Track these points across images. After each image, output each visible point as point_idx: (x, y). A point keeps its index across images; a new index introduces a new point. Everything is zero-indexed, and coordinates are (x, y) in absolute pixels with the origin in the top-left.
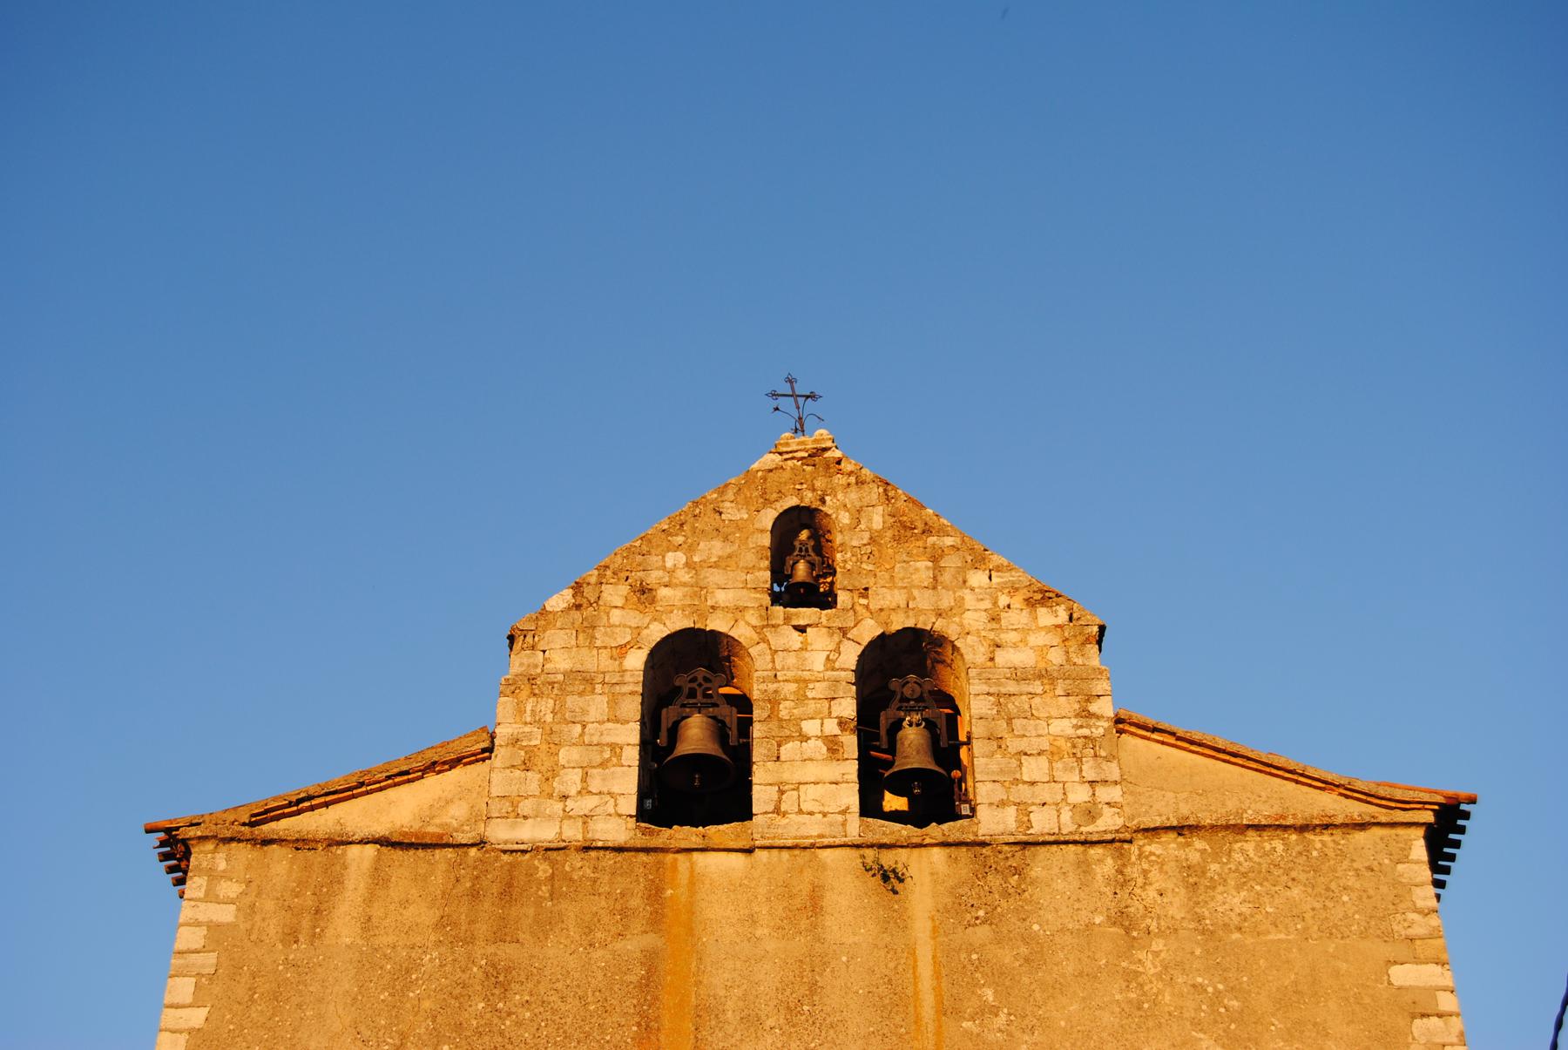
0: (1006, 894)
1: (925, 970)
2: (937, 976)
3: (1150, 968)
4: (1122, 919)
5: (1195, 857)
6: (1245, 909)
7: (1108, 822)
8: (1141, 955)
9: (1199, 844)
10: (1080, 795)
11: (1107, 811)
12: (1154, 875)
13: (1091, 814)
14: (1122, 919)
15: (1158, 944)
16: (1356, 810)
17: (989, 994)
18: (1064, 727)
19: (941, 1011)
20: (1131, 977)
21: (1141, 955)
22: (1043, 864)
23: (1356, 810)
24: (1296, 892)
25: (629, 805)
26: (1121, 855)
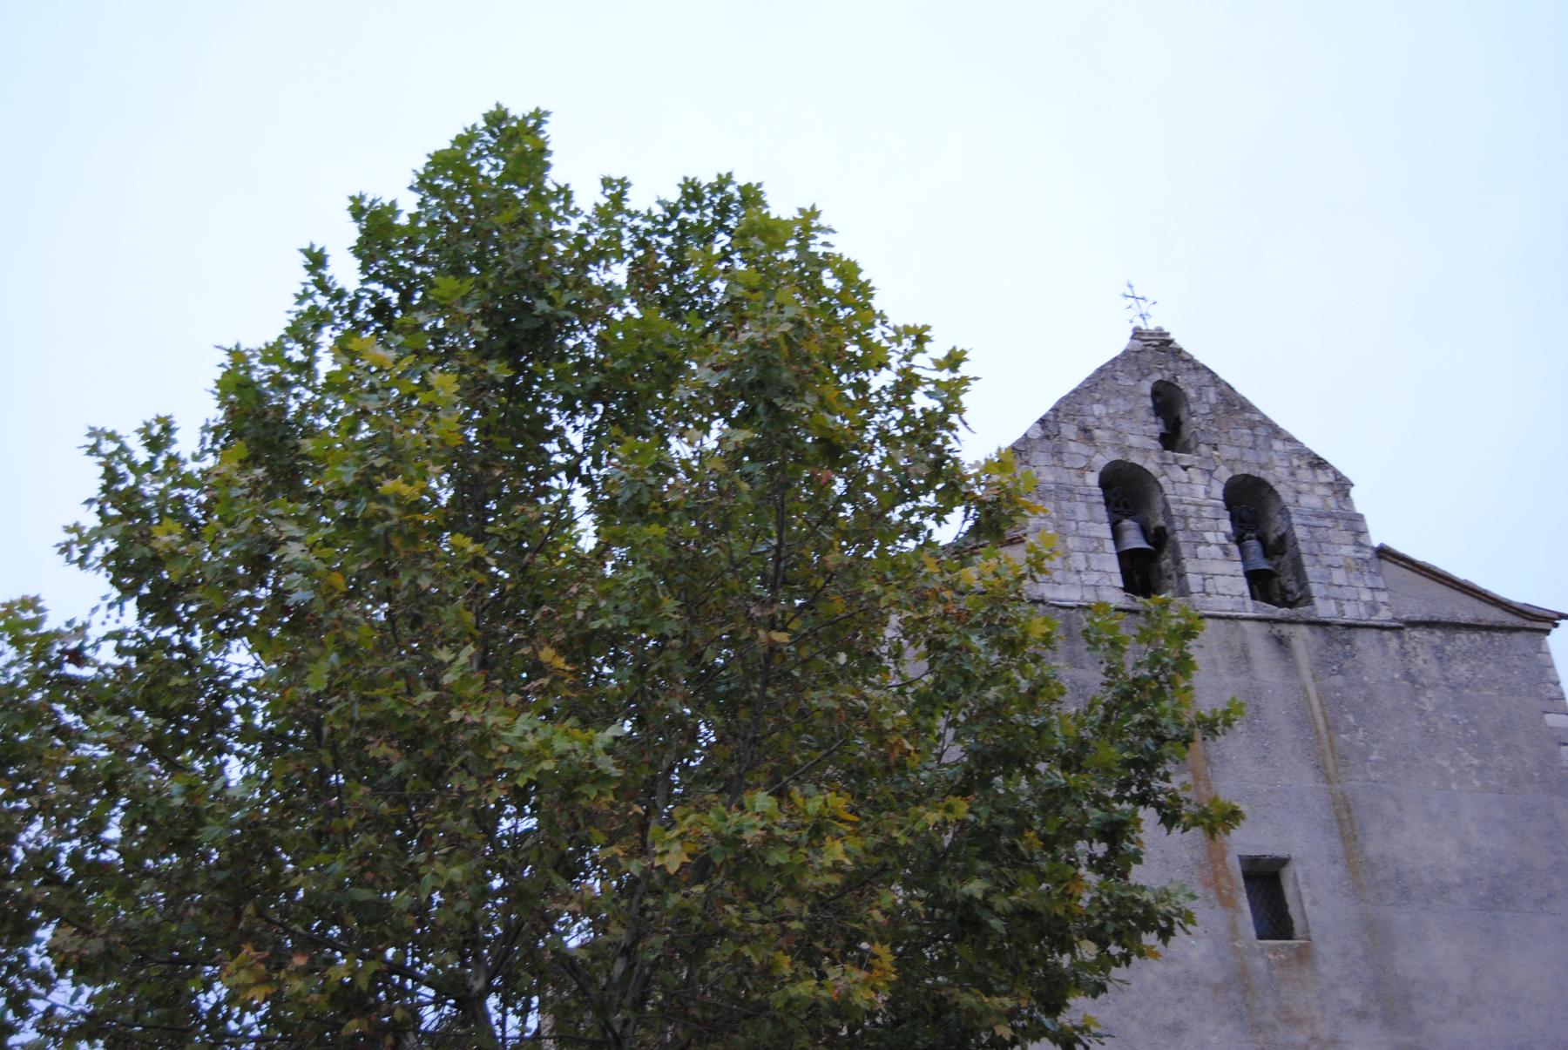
0: (1345, 657)
1: (1317, 710)
2: (1322, 705)
3: (1429, 708)
4: (1408, 675)
5: (1438, 642)
6: (1468, 674)
7: (1384, 615)
8: (1423, 699)
9: (1438, 633)
10: (1366, 596)
11: (1384, 608)
12: (1419, 650)
13: (1374, 608)
14: (1408, 675)
15: (1430, 694)
16: (1511, 620)
17: (1351, 718)
18: (1348, 550)
19: (1328, 728)
20: (1421, 712)
21: (1423, 699)
22: (1363, 640)
23: (1511, 620)
24: (1491, 667)
25: (1253, 933)
26: (1400, 637)
